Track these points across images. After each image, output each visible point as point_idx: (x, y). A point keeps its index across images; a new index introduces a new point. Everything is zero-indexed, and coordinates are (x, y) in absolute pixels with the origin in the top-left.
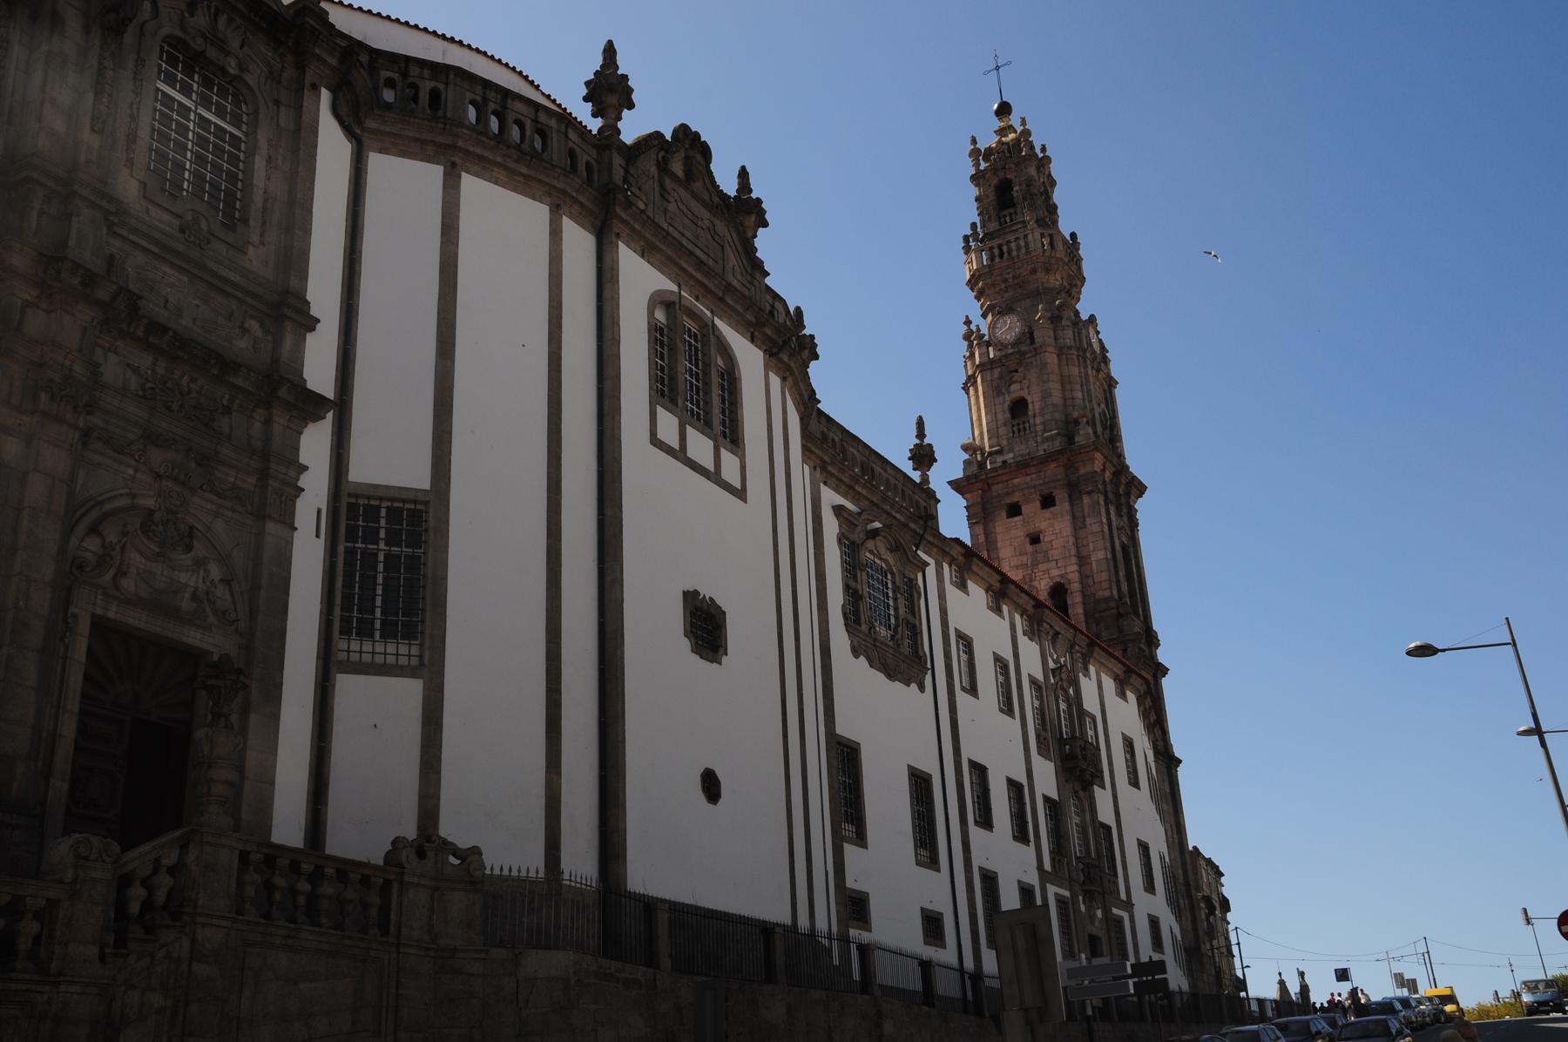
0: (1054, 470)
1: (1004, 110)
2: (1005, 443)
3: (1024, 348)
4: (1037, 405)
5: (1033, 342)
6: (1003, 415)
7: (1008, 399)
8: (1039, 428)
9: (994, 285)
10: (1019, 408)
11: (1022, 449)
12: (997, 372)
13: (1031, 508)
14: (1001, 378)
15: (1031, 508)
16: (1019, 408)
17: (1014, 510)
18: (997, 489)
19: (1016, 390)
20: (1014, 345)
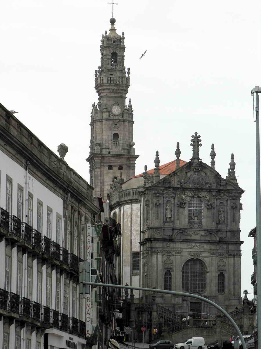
0: (123, 161)
1: (113, 21)
2: (110, 146)
3: (120, 118)
4: (122, 138)
5: (123, 117)
6: (111, 137)
7: (113, 132)
8: (121, 145)
9: (109, 89)
10: (116, 136)
11: (114, 151)
12: (111, 122)
13: (115, 169)
14: (112, 125)
15: (115, 169)
16: (116, 136)
17: (110, 167)
18: (106, 160)
19: (116, 131)
20: (117, 116)
